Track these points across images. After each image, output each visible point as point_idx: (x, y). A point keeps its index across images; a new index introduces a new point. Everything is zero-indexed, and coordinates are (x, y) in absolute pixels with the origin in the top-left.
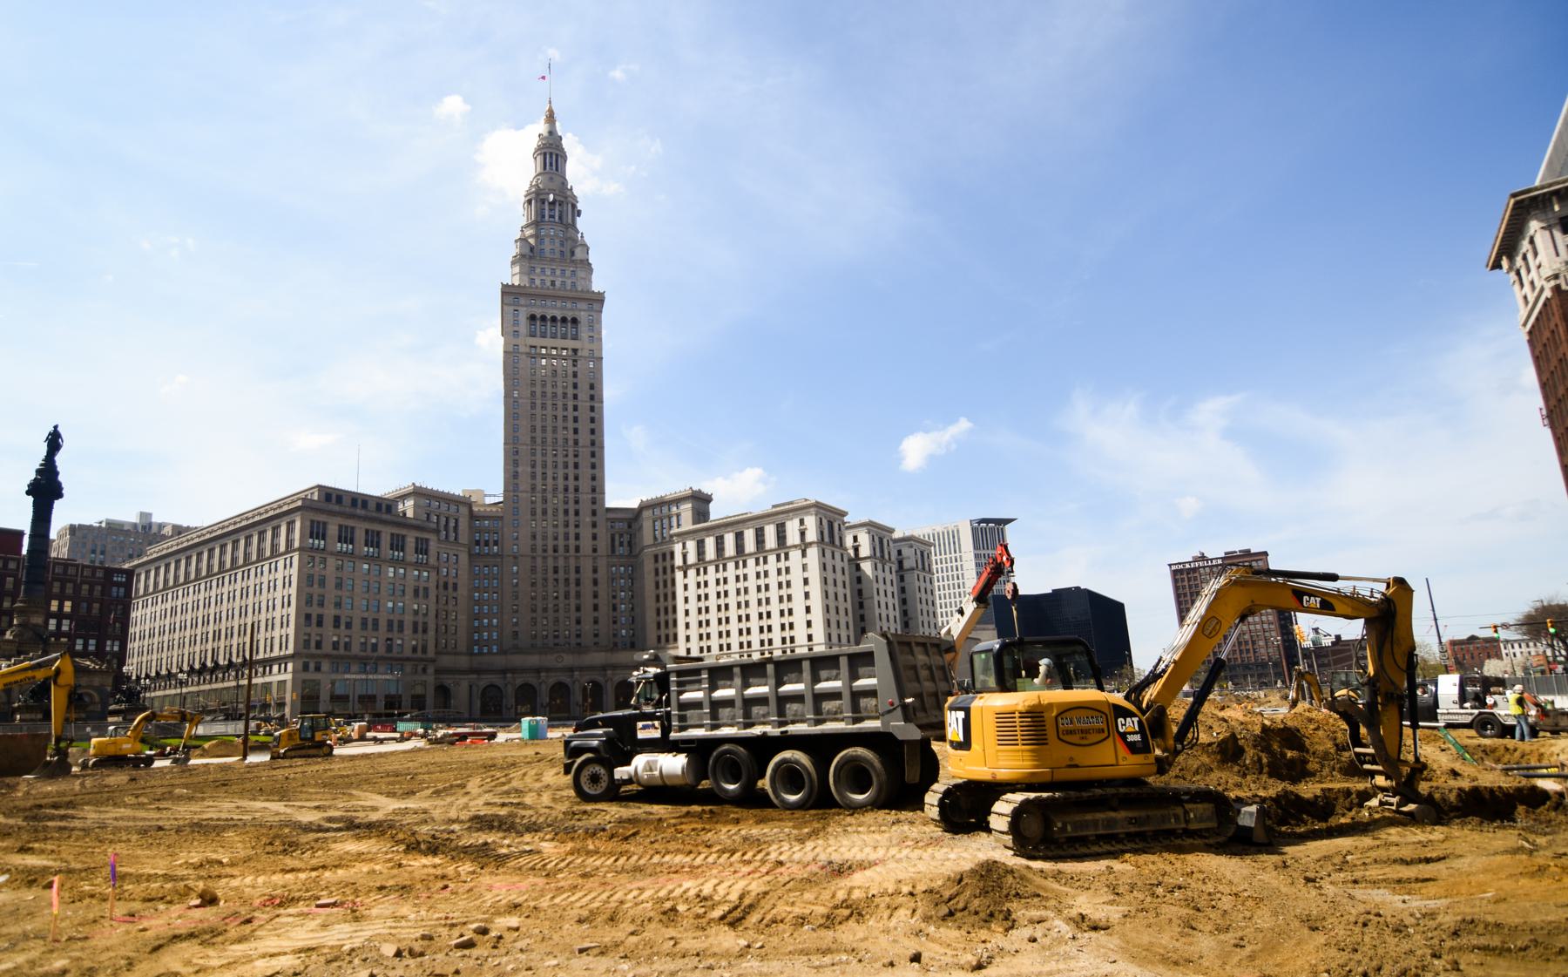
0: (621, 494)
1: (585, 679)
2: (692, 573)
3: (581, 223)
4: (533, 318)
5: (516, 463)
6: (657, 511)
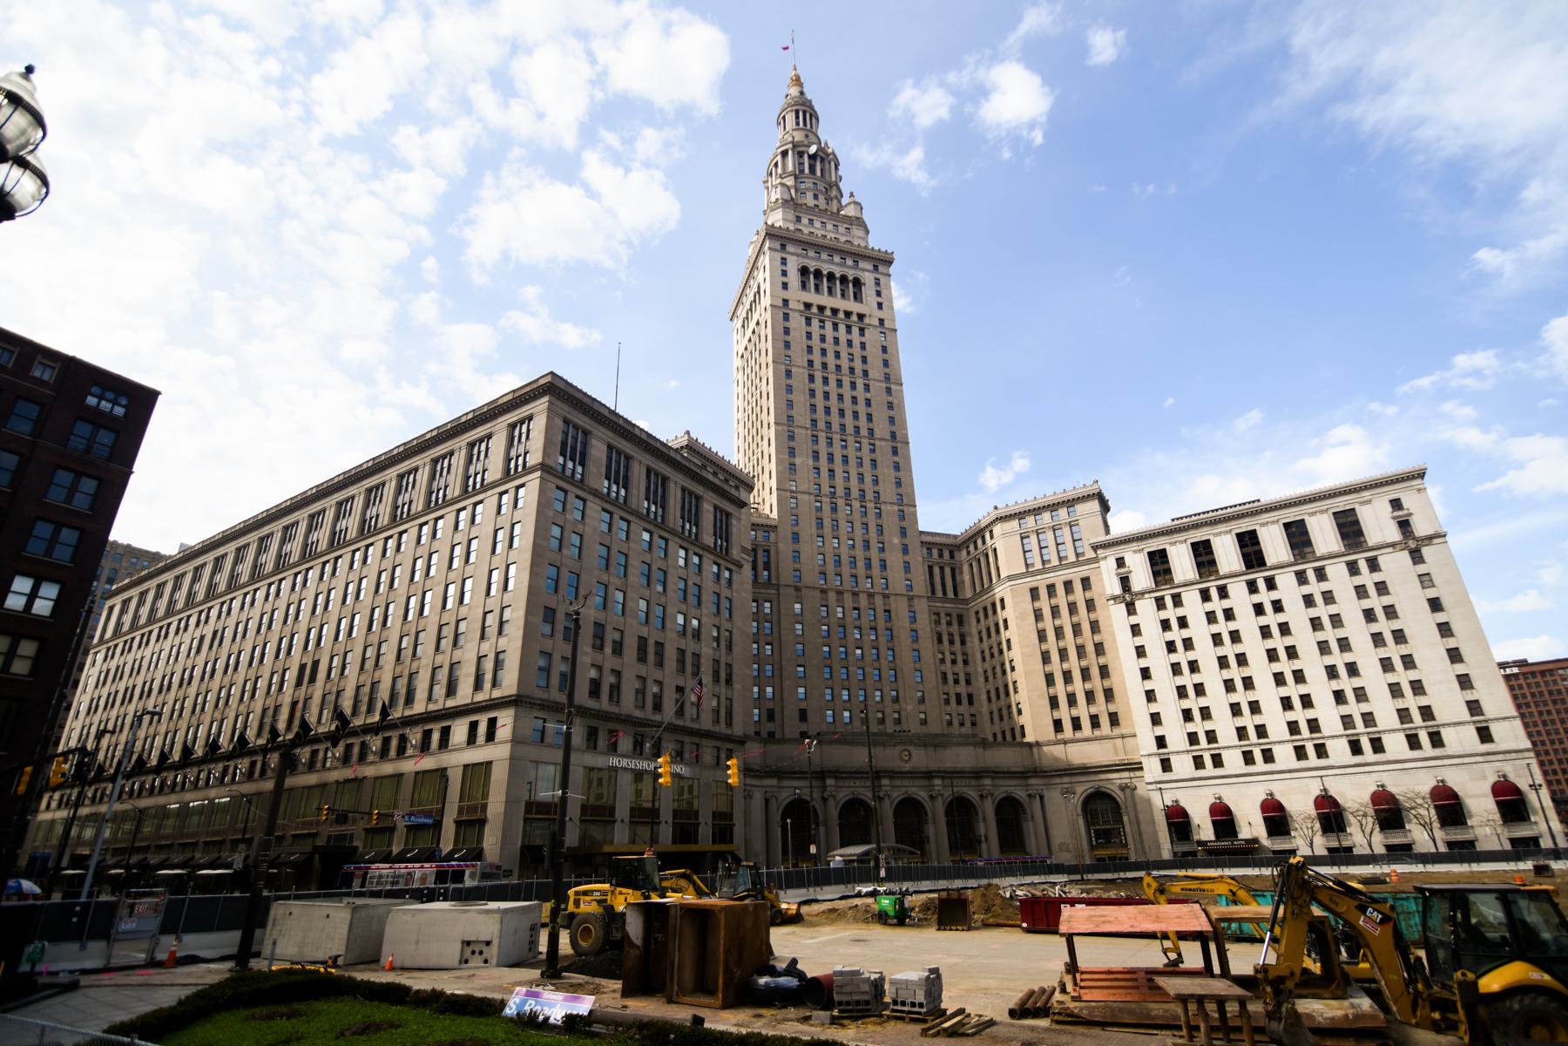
2: (1145, 606)
4: (804, 271)
5: (792, 452)
6: (1030, 521)
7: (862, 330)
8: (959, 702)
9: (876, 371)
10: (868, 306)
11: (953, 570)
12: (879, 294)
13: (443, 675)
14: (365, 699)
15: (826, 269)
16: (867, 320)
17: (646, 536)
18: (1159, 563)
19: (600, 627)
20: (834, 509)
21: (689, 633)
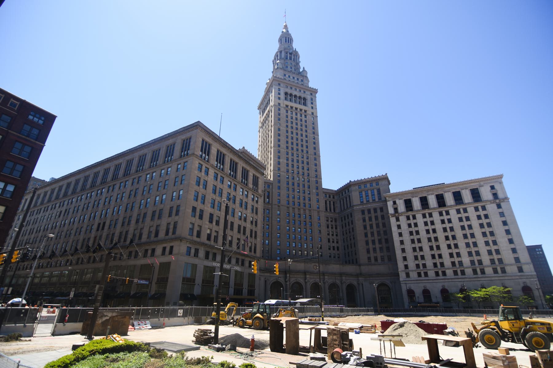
0: (332, 179)
1: (329, 280)
2: (403, 219)
3: (302, 65)
4: (286, 94)
5: (279, 158)
7: (306, 116)
8: (334, 249)
9: (310, 131)
10: (308, 108)
11: (334, 202)
12: (312, 103)
13: (153, 229)
14: (123, 237)
15: (294, 93)
16: (308, 112)
17: (229, 183)
18: (408, 204)
19: (211, 216)
20: (293, 179)
21: (243, 218)
